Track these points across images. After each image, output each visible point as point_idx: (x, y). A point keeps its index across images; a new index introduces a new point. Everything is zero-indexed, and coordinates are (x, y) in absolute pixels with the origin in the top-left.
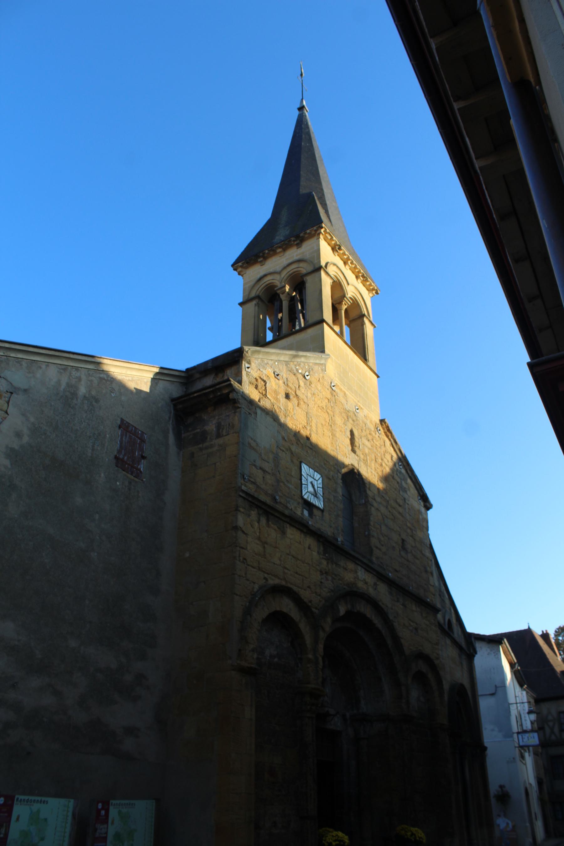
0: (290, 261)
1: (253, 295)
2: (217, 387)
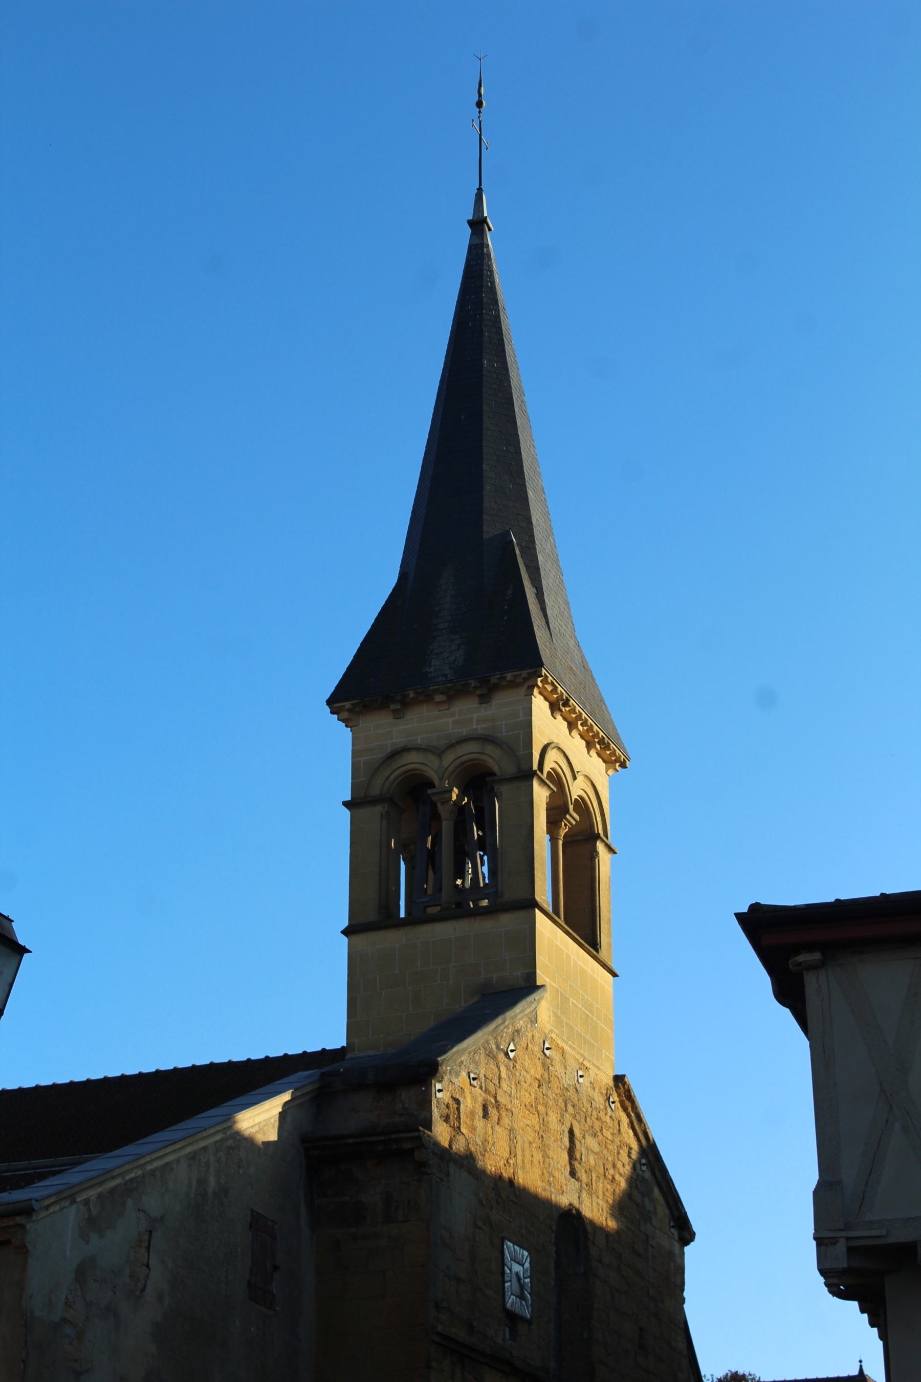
0: (464, 731)
1: (375, 791)
2: (394, 1136)
